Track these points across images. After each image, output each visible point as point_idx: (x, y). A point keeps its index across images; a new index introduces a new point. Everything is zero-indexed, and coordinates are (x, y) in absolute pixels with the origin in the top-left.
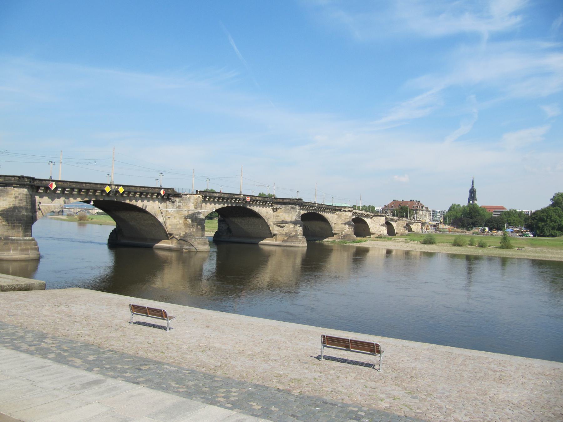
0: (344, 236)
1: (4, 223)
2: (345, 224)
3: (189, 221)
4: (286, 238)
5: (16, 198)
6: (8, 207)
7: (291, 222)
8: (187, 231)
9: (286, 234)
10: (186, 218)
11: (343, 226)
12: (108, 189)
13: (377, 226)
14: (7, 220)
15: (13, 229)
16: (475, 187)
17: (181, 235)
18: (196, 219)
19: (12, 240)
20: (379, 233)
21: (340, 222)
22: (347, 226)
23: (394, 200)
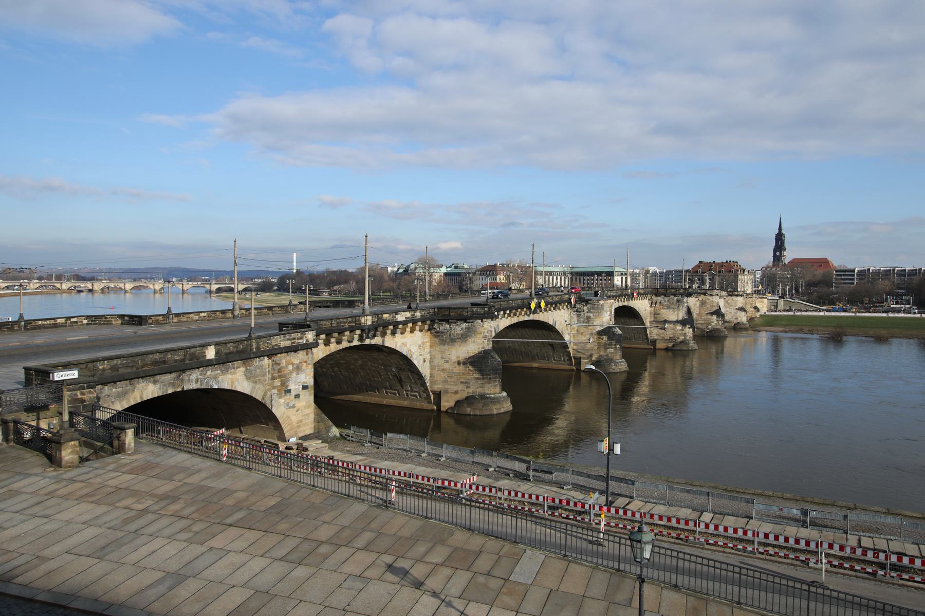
0: (711, 331)
1: (476, 376)
2: (712, 314)
3: (605, 338)
4: (670, 345)
5: (485, 337)
6: (477, 352)
7: (677, 322)
8: (602, 353)
9: (670, 339)
10: (600, 333)
11: (709, 317)
12: (533, 306)
13: (733, 311)
14: (481, 371)
15: (489, 383)
16: (783, 232)
17: (594, 358)
18: (614, 334)
19: (494, 398)
20: (736, 321)
21: (704, 312)
22: (715, 317)
23: (700, 262)
